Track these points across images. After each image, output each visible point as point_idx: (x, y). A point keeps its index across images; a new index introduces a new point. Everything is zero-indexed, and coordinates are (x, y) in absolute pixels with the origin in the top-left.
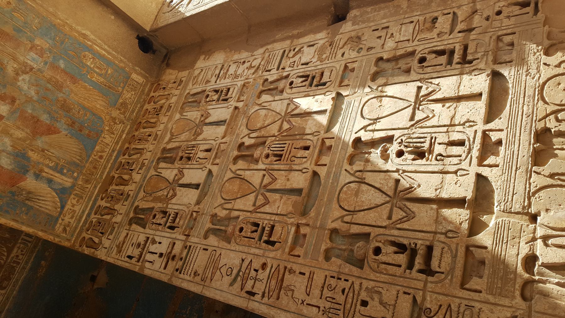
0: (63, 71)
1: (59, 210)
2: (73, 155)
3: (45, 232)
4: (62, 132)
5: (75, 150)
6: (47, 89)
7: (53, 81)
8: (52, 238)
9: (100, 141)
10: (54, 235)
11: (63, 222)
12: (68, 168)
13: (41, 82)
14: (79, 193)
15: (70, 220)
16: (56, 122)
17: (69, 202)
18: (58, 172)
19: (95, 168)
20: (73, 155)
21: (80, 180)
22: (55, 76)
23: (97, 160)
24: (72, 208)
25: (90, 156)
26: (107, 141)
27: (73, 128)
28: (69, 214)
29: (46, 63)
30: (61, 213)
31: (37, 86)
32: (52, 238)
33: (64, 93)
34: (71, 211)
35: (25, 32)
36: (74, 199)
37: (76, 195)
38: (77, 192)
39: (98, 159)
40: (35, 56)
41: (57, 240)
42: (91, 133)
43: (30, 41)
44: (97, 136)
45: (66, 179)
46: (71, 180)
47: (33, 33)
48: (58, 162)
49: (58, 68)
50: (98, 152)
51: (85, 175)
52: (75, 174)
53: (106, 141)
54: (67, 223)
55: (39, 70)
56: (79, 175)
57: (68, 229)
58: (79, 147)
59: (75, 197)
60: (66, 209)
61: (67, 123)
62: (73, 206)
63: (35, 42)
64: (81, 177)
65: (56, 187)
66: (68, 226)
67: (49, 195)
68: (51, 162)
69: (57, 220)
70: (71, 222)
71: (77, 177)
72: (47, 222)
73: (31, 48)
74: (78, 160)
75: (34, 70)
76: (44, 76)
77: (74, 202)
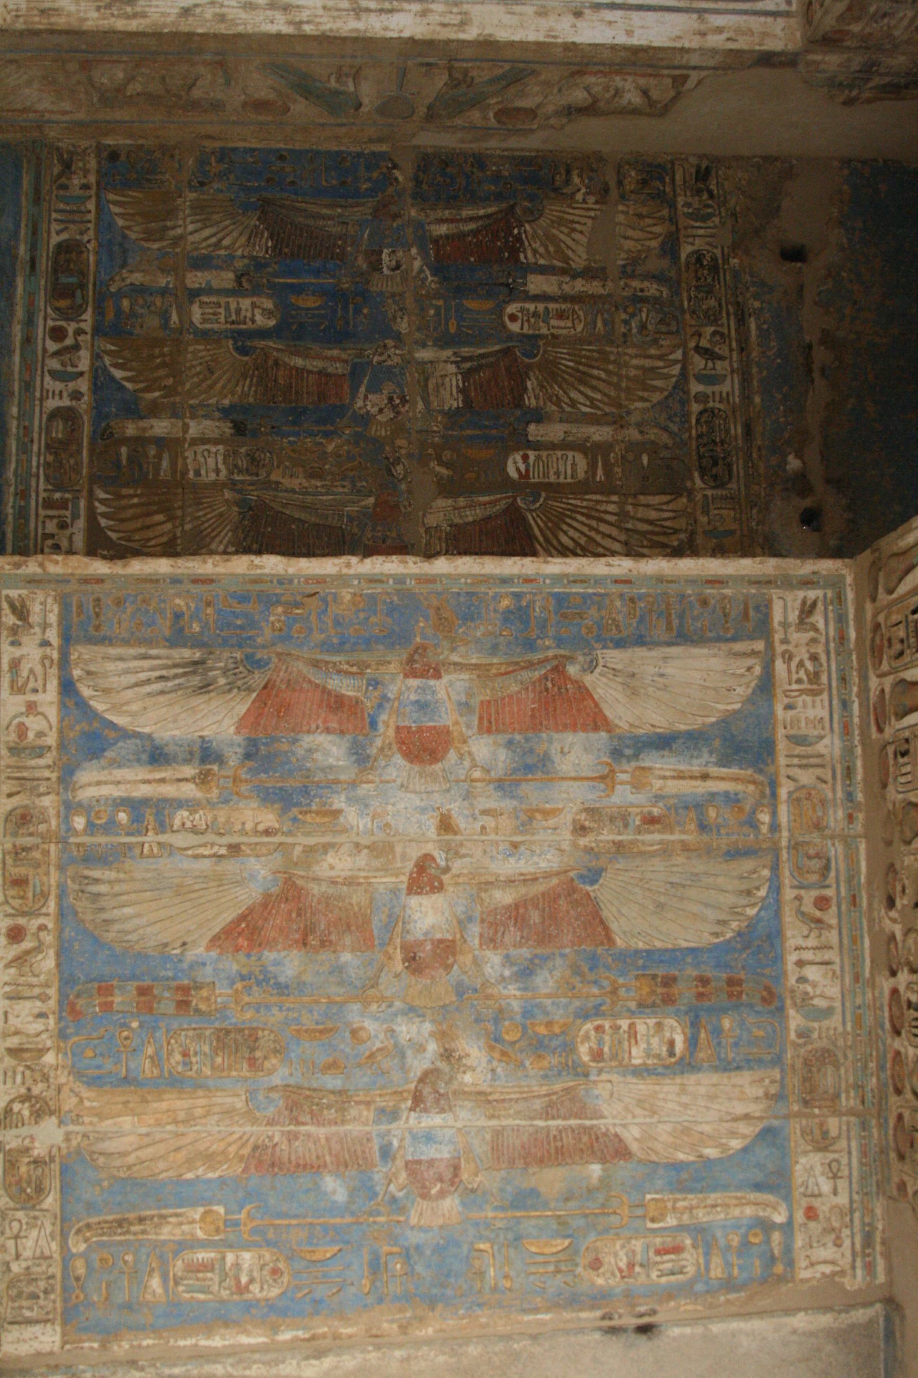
0: (315, 1168)
1: (77, 673)
2: (124, 887)
3: (86, 581)
4: (208, 949)
5: (127, 911)
6: (332, 1066)
7: (329, 1107)
8: (52, 569)
9: (52, 992)
10: (49, 581)
11: (39, 636)
12: (118, 834)
13: (366, 1079)
14: (33, 763)
15: (17, 652)
16: (245, 971)
17: (53, 714)
18: (145, 802)
19: (20, 882)
20: (124, 887)
21: (52, 812)
22: (334, 1129)
23: (24, 914)
24: (32, 697)
25: (61, 914)
26: (27, 1008)
27: (173, 984)
28: (31, 671)
29: (386, 1153)
30: (64, 663)
31: (371, 1056)
32: (52, 569)
33: (272, 1089)
34: (31, 685)
35: (503, 1208)
36: (40, 734)
37: (40, 751)
38: (42, 762)
39: (21, 921)
40: (429, 1152)
41: (32, 567)
42: (100, 1005)
43: (473, 1191)
44: (72, 1006)
45: (105, 791)
46: (86, 794)
47: (477, 1224)
48: (163, 838)
49: (341, 1165)
50: (38, 949)
51: (46, 838)
52: (79, 822)
53: (28, 1004)
54: (25, 639)
55: (394, 1115)
56: (63, 827)
57: (10, 619)
58: (117, 927)
59: (39, 742)
60: (53, 685)
61: (204, 993)
62: (31, 707)
63: (457, 1201)
64: (54, 823)
65: (125, 748)
66: (14, 631)
67: (134, 707)
68: (188, 824)
69: (67, 639)
70: (12, 649)
71: (66, 817)
72: (97, 615)
73: (456, 1168)
74: (97, 881)
75: (409, 1103)
76: (368, 1104)
77: (34, 724)
